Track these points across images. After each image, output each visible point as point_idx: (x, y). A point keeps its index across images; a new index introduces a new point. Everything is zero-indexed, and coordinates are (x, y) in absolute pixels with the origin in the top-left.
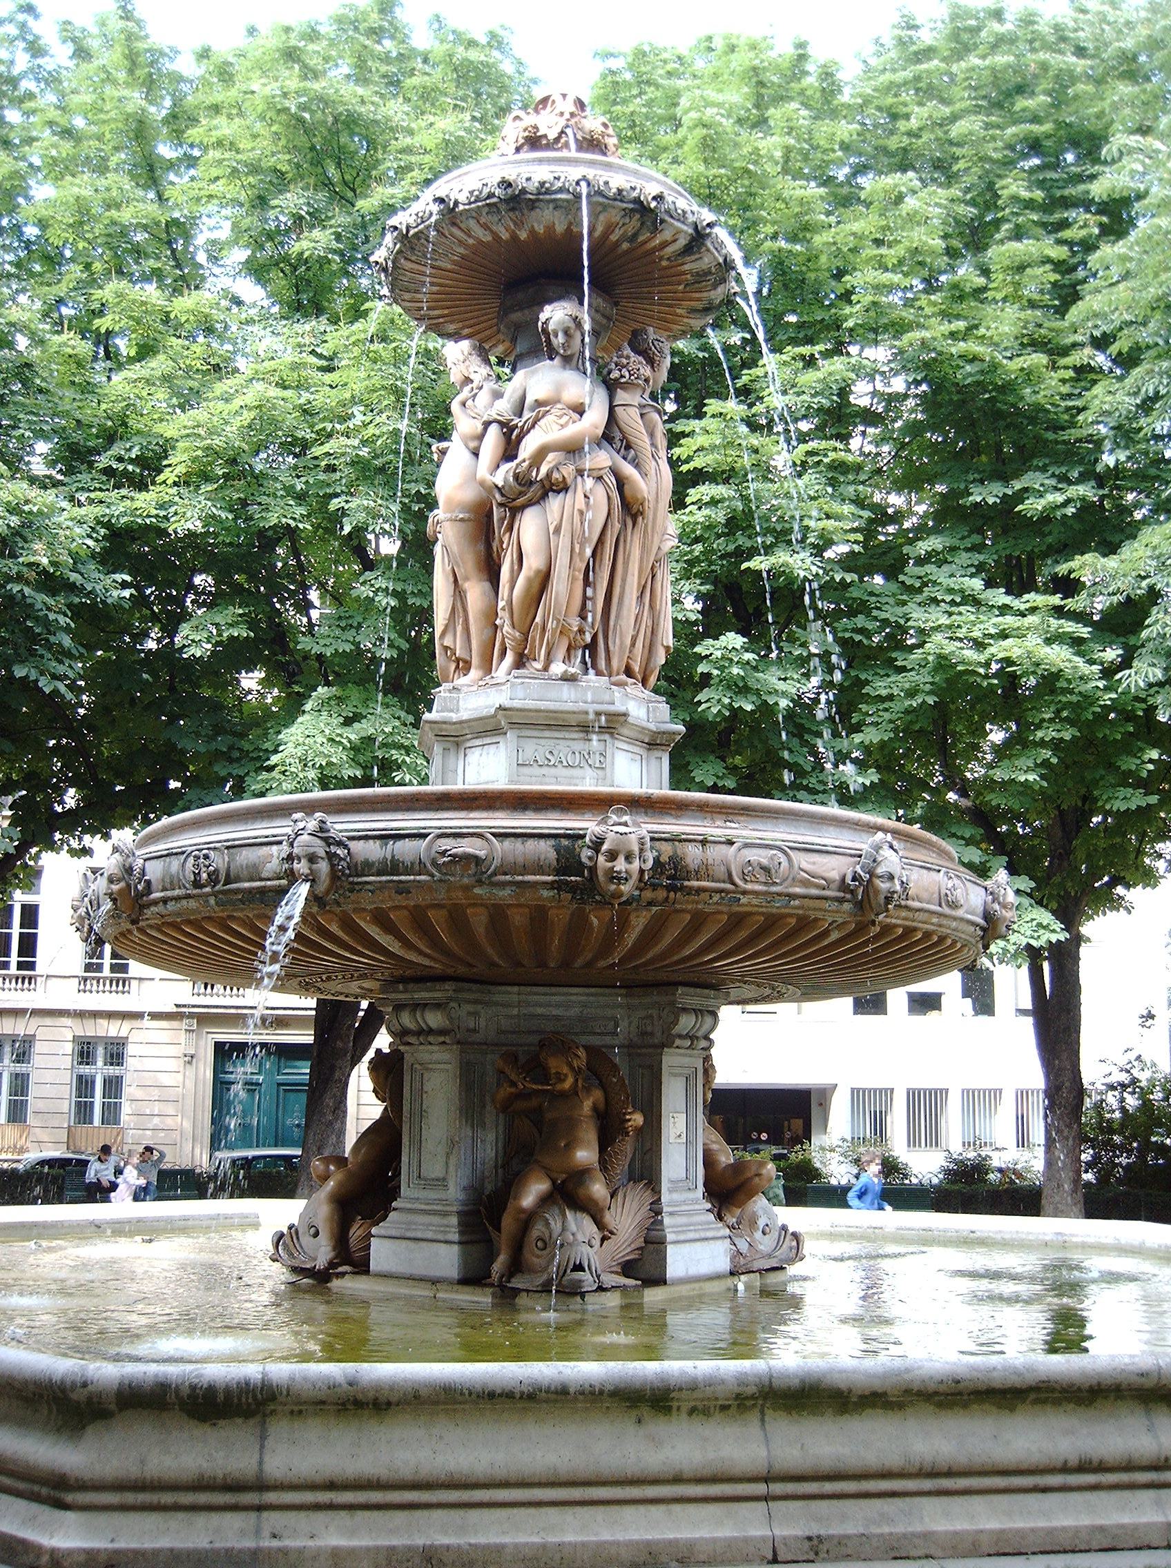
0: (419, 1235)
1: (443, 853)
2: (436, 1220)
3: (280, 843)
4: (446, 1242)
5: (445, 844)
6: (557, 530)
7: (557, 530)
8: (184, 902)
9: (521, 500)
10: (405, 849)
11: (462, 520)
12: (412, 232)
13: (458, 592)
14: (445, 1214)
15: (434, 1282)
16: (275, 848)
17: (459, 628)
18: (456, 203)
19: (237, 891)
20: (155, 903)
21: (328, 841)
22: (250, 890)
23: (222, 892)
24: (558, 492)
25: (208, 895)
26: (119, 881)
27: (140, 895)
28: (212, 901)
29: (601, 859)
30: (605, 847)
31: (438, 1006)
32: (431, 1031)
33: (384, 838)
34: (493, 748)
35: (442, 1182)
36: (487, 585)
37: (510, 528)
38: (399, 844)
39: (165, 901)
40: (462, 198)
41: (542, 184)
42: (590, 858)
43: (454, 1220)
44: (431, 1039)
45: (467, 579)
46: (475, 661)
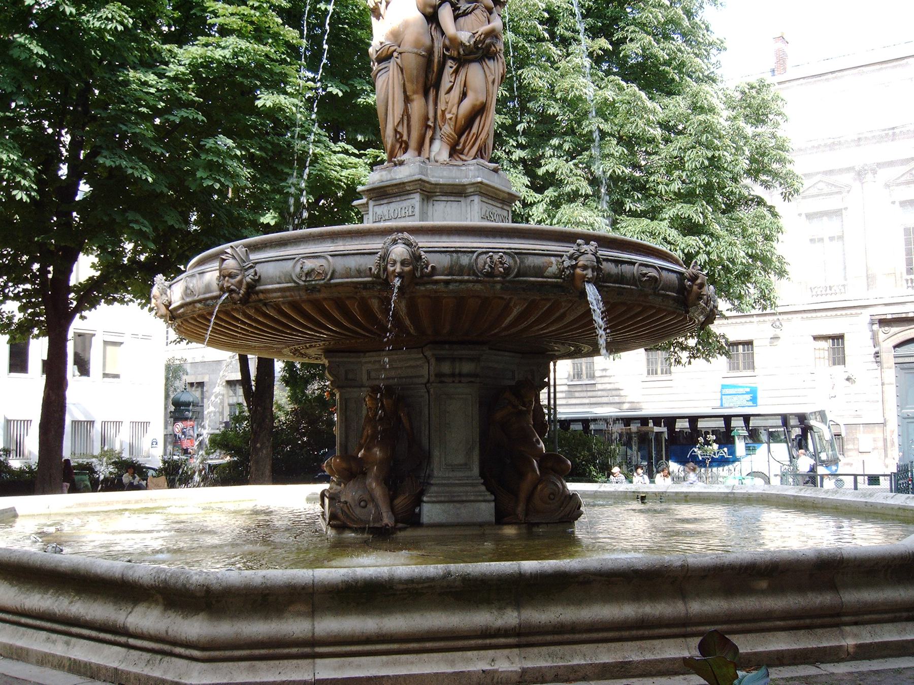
0: (464, 499)
1: (644, 275)
2: (469, 489)
3: (562, 256)
4: (485, 501)
5: (645, 270)
6: (493, 82)
7: (493, 82)
8: (470, 285)
9: (472, 57)
10: (626, 268)
11: (423, 56)
13: (407, 100)
14: (473, 485)
15: (481, 525)
16: (553, 259)
17: (405, 122)
19: (525, 282)
20: (437, 282)
21: (597, 258)
22: (533, 283)
23: (509, 282)
24: (489, 59)
25: (498, 282)
26: (409, 264)
27: (423, 275)
28: (498, 286)
29: (695, 288)
30: (699, 281)
31: (471, 359)
32: (460, 375)
33: (618, 262)
34: (455, 204)
35: (466, 466)
36: (423, 100)
37: (456, 72)
38: (623, 266)
39: (447, 283)
42: (690, 286)
43: (483, 488)
44: (463, 379)
45: (415, 92)
46: (413, 143)
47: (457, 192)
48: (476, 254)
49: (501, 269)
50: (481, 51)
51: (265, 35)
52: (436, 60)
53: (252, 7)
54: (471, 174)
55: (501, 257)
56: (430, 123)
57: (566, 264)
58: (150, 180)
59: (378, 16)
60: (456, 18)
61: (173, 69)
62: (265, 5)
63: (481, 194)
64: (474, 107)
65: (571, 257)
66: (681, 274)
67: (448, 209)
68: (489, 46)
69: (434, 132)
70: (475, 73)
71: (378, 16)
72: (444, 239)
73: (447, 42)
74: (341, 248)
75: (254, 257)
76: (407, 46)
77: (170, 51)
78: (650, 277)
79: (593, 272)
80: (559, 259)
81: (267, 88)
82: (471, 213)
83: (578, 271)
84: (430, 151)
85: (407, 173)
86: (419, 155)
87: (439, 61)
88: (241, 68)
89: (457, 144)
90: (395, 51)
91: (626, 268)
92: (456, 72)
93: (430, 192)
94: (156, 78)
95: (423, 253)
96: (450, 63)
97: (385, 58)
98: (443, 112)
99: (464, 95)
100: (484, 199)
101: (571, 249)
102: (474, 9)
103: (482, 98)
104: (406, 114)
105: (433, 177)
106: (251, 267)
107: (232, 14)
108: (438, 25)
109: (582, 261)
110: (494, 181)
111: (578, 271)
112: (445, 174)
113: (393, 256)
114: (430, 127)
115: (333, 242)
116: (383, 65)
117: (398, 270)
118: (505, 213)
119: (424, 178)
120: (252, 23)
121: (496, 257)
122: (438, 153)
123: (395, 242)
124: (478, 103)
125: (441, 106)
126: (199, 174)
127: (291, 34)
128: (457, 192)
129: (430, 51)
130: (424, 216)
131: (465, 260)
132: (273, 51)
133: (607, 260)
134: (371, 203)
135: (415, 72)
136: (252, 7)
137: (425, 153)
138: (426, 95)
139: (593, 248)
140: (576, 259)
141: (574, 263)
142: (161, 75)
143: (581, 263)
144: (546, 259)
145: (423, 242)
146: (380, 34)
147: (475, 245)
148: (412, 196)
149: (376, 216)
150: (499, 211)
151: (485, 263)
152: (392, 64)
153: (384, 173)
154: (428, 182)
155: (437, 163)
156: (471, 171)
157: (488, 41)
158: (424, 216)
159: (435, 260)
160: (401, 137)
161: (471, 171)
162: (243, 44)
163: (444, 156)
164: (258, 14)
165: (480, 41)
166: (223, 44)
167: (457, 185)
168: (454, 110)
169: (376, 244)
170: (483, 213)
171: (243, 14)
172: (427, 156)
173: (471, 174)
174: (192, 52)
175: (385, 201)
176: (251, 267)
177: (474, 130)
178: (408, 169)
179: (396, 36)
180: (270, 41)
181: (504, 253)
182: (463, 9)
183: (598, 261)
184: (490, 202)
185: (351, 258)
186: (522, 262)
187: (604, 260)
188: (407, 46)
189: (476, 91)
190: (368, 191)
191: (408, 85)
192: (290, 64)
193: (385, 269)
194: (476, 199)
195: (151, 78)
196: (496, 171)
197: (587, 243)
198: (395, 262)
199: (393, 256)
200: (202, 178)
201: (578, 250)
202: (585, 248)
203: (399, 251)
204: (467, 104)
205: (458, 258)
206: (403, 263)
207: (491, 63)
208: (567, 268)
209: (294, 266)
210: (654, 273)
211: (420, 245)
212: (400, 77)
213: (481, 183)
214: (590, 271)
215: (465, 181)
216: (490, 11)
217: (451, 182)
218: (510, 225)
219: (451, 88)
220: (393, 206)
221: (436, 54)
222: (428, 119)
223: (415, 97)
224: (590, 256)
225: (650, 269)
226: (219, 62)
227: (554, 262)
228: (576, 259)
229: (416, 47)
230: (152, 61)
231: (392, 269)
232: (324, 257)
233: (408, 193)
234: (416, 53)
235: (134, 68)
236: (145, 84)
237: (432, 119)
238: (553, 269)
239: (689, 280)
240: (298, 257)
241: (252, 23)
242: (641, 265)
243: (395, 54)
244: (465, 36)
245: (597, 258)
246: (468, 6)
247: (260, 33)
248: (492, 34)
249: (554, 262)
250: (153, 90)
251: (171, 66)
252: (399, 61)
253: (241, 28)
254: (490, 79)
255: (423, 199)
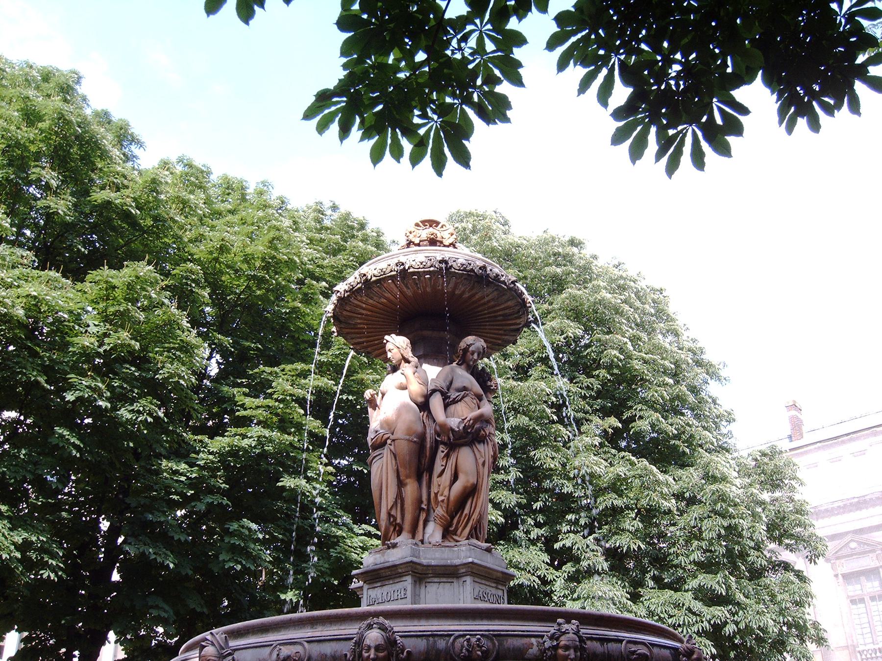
1: (634, 652)
3: (542, 637)
5: (633, 648)
6: (484, 464)
7: (484, 464)
11: (415, 442)
12: (411, 270)
13: (401, 484)
16: (533, 640)
17: (399, 505)
18: (451, 266)
21: (580, 637)
24: (479, 442)
33: (604, 640)
37: (447, 456)
38: (610, 645)
40: (454, 264)
41: (497, 275)
45: (408, 477)
46: (407, 526)
47: (449, 573)
48: (452, 638)
49: (479, 653)
50: (472, 435)
51: (289, 425)
52: (428, 446)
53: (277, 400)
54: (463, 554)
55: (479, 640)
56: (423, 506)
57: (547, 645)
58: (172, 566)
59: (375, 406)
60: (446, 406)
61: (203, 458)
62: (288, 398)
63: (473, 574)
64: (465, 488)
65: (552, 638)
66: (676, 649)
67: (441, 590)
68: (479, 430)
69: (428, 515)
70: (465, 457)
71: (375, 406)
72: (423, 622)
73: (438, 428)
74: (318, 634)
75: (233, 643)
76: (399, 434)
77: (201, 441)
78: (640, 654)
79: (575, 651)
80: (540, 640)
81: (290, 474)
82: (463, 595)
83: (560, 651)
84: (424, 533)
85: (400, 556)
86: (413, 538)
87: (431, 447)
88: (264, 455)
89: (450, 525)
90: (388, 438)
91: (612, 646)
92: (447, 456)
93: (422, 574)
94: (187, 467)
95: (398, 638)
96: (441, 448)
97: (380, 445)
98: (436, 494)
99: (455, 477)
100: (476, 579)
101: (552, 629)
102: (463, 397)
103: (473, 480)
104: (400, 497)
105: (425, 558)
106: (230, 654)
107: (258, 407)
108: (430, 412)
109: (563, 641)
110: (488, 561)
111: (560, 651)
112: (437, 555)
113: (367, 642)
114: (424, 509)
115: (312, 628)
116: (377, 452)
117: (372, 656)
118: (500, 593)
119: (415, 559)
120: (277, 415)
121: (473, 640)
122: (432, 535)
123: (370, 627)
124: (469, 485)
125: (434, 489)
126: (221, 557)
127: (312, 424)
128: (449, 573)
129: (422, 437)
130: (416, 599)
131: (441, 644)
132: (296, 440)
133: (591, 639)
134: (366, 587)
135: (407, 458)
136: (277, 400)
137: (419, 536)
138: (419, 479)
139: (574, 627)
140: (557, 639)
141: (555, 643)
142: (191, 465)
143: (562, 643)
144: (525, 641)
145: (399, 626)
146: (376, 420)
147: (452, 628)
148: (404, 579)
149: (374, 598)
150: (494, 591)
151: (462, 646)
152: (386, 451)
153: (378, 556)
154: (419, 564)
155: (431, 546)
156: (464, 552)
157: (477, 426)
158: (416, 599)
159: (410, 645)
160: (395, 519)
161: (464, 552)
162: (267, 433)
163: (437, 537)
164: (281, 406)
165: (469, 426)
166: (249, 435)
167: (449, 566)
168: (446, 493)
169: (351, 630)
170: (476, 593)
171: (268, 406)
172: (421, 538)
173: (463, 554)
174: (219, 443)
175: (379, 584)
176: (230, 654)
177: (466, 511)
178: (402, 551)
179: (388, 425)
180: (293, 430)
181: (482, 635)
182: (453, 397)
183: (581, 640)
184: (483, 582)
185: (327, 644)
186: (500, 644)
187: (588, 639)
188: (399, 434)
189: (466, 474)
190: (362, 574)
191: (401, 470)
192: (313, 451)
193: (360, 655)
194: (468, 579)
195: (183, 467)
196: (488, 550)
197: (568, 622)
198: (369, 648)
199: (367, 642)
200: (224, 561)
201: (559, 630)
202: (566, 627)
203: (374, 636)
204: (458, 486)
205: (435, 642)
206: (378, 648)
207: (481, 447)
208: (548, 649)
209: (271, 653)
210: (643, 650)
211: (395, 629)
212: (394, 462)
213: (472, 563)
214: (572, 651)
215: (457, 562)
216: (479, 398)
217: (442, 563)
218: (505, 606)
219: (443, 471)
220: (386, 589)
221: (428, 440)
222: (422, 502)
223: (408, 481)
224: (571, 635)
225: (640, 647)
226: (245, 451)
227: (535, 643)
228: (557, 639)
229: (409, 435)
230: (182, 451)
231: (366, 655)
232: (300, 644)
233: (401, 575)
234: (408, 440)
235: (168, 459)
236: (176, 472)
237: (425, 502)
238: (534, 650)
239: (684, 656)
240: (275, 643)
241: (277, 415)
242: (629, 642)
243: (389, 441)
244: (454, 422)
245: (580, 637)
246: (458, 394)
247: (284, 424)
248: (482, 419)
249: (535, 643)
250: (183, 479)
251: (201, 455)
252: (392, 447)
253: (267, 419)
254: (481, 461)
255: (415, 581)
